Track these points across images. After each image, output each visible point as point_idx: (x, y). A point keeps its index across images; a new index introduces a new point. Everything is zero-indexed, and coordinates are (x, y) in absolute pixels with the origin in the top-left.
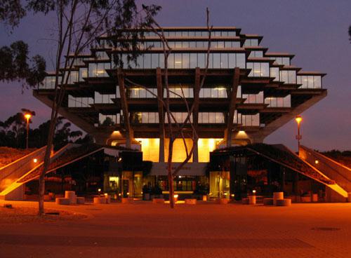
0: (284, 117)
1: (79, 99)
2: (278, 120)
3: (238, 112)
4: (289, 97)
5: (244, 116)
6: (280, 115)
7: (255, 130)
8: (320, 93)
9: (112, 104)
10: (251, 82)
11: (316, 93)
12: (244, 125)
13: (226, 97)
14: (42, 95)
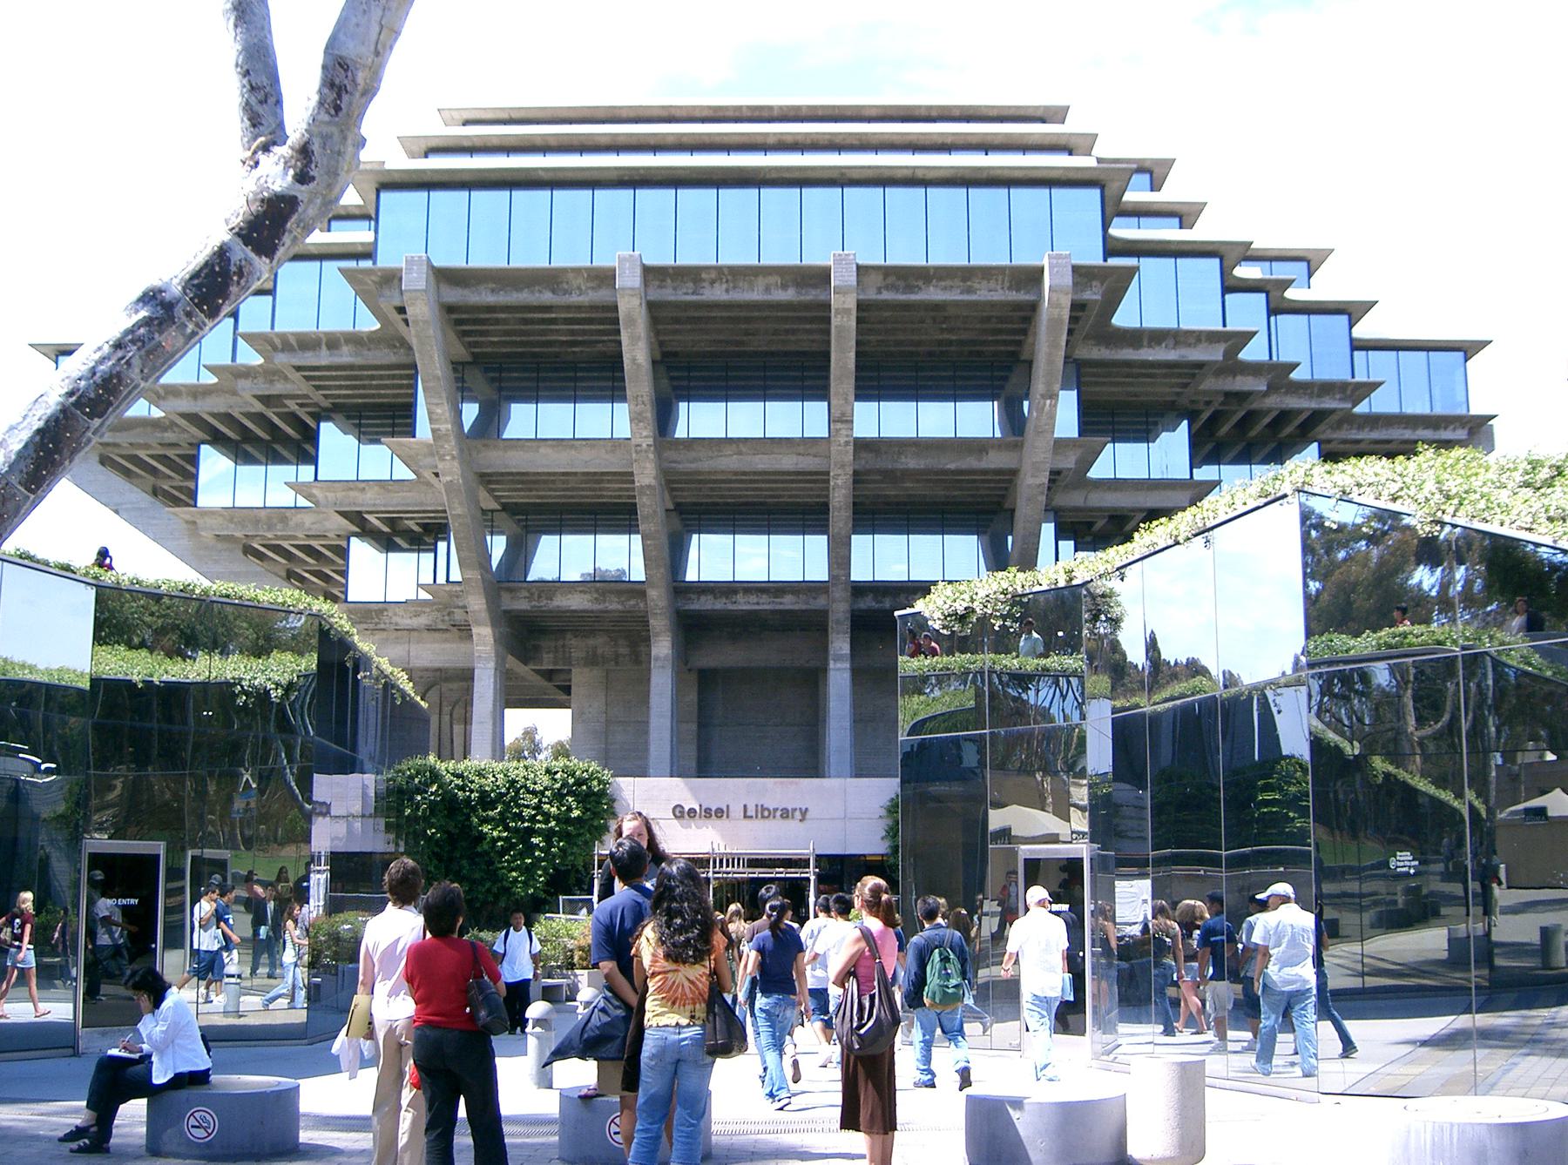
1: (252, 474)
3: (1060, 535)
8: (1461, 434)
10: (1127, 354)
13: (998, 435)
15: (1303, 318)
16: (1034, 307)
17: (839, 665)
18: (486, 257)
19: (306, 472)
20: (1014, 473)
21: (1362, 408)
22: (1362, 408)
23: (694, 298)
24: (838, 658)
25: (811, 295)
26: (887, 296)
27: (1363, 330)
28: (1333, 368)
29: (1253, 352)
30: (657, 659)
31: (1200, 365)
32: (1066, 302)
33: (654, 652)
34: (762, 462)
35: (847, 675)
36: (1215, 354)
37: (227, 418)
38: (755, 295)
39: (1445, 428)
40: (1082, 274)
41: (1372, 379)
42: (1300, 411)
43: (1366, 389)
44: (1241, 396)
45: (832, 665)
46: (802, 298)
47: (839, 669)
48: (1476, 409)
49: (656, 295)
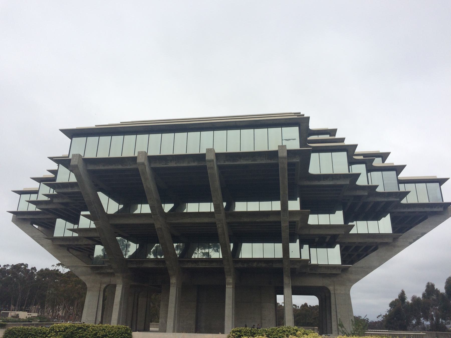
0: (381, 251)
2: (373, 257)
4: (387, 218)
5: (313, 250)
6: (376, 249)
7: (334, 272)
8: (441, 209)
9: (93, 229)
11: (435, 210)
12: (313, 262)
14: (24, 220)
15: (380, 173)
16: (277, 165)
17: (229, 286)
18: (103, 154)
19: (76, 227)
20: (280, 222)
21: (404, 201)
22: (404, 201)
23: (167, 166)
24: (229, 284)
25: (202, 164)
26: (227, 163)
27: (403, 175)
28: (392, 187)
29: (362, 181)
30: (172, 283)
31: (342, 186)
32: (286, 162)
33: (171, 281)
34: (198, 220)
35: (231, 290)
36: (347, 182)
37: (54, 209)
38: (185, 164)
39: (435, 208)
40: (291, 153)
41: (407, 190)
42: (382, 202)
43: (406, 194)
44: (360, 197)
45: (227, 286)
46: (200, 165)
47: (229, 288)
48: (446, 200)
49: (153, 165)
